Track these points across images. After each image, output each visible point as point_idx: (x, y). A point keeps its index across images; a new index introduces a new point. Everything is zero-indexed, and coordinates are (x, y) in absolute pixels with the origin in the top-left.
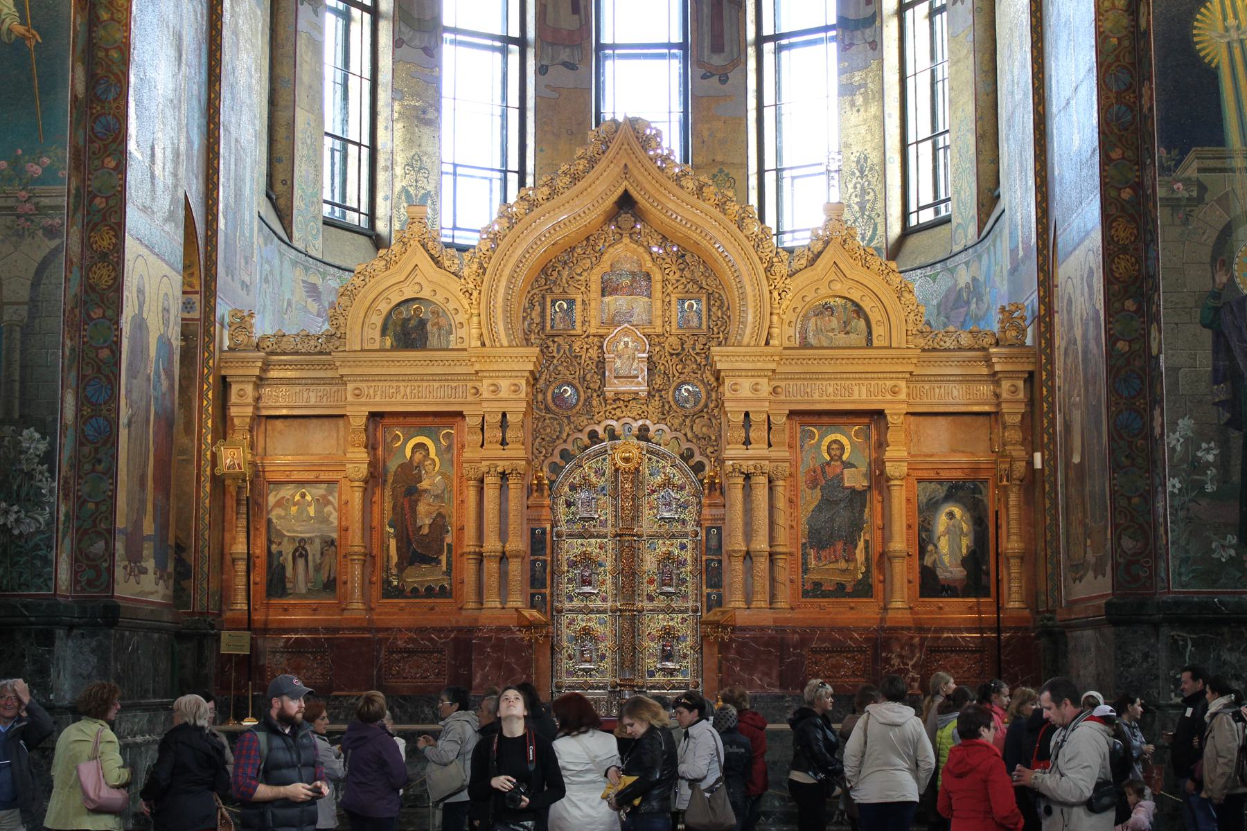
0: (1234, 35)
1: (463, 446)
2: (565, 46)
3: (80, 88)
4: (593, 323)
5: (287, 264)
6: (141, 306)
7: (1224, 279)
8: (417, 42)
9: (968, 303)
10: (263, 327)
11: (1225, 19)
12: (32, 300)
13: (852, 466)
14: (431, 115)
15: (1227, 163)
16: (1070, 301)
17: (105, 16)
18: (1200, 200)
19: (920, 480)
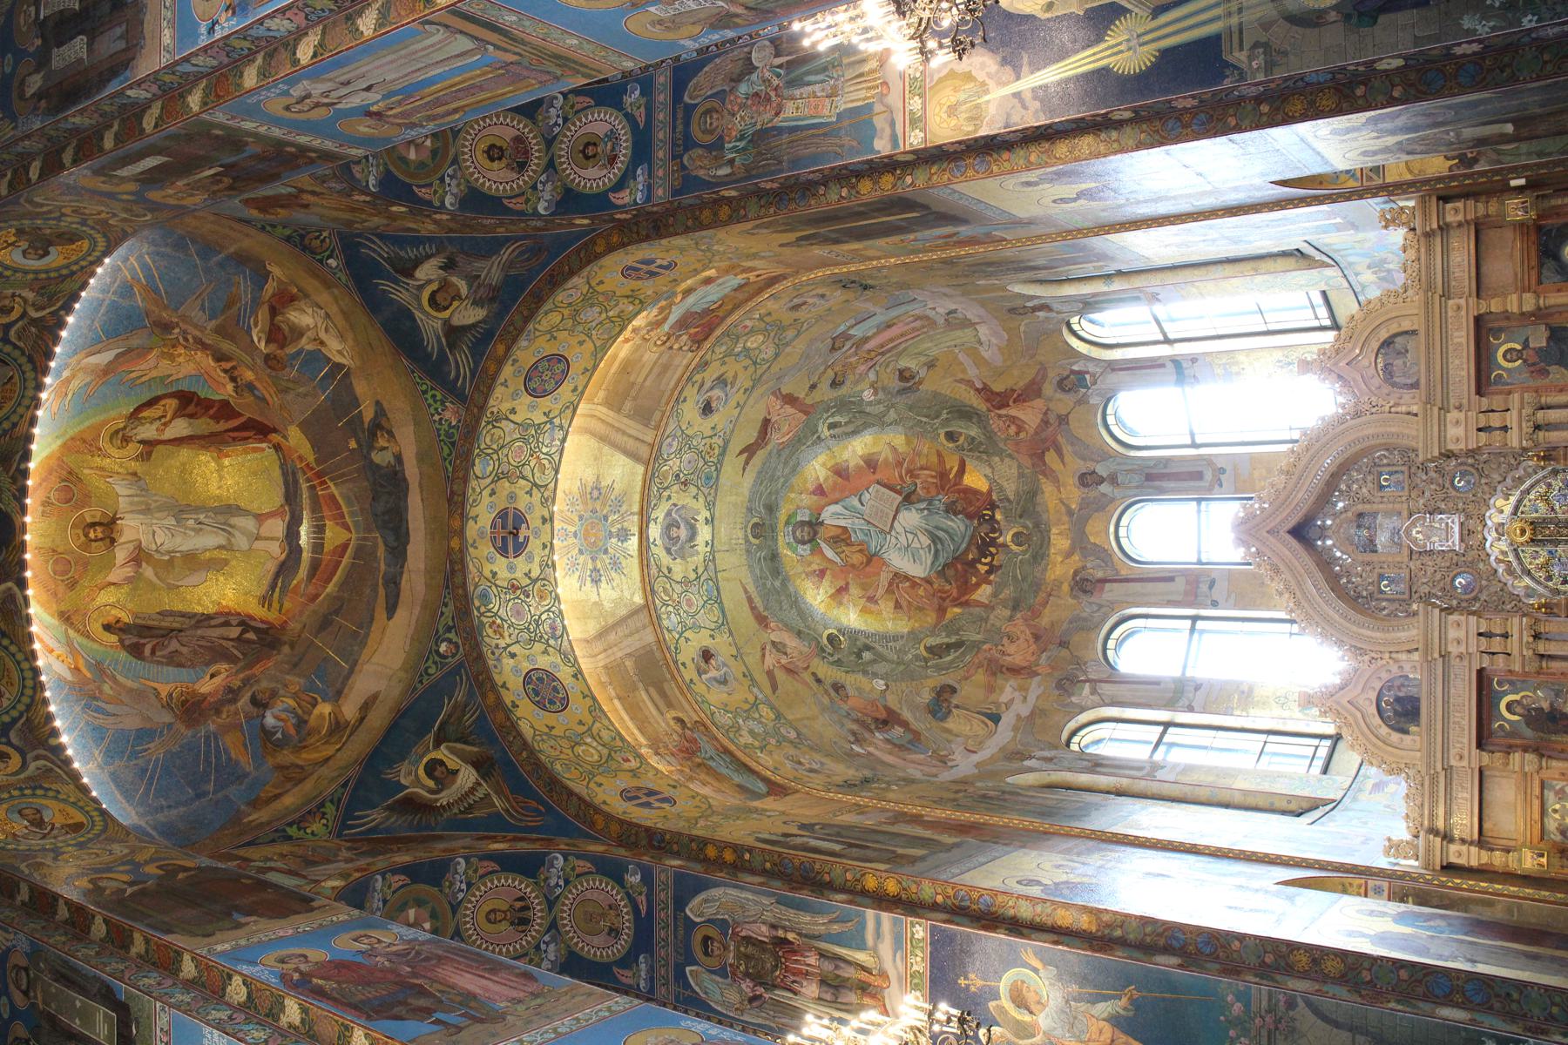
0: (1134, 43)
1: (1510, 671)
2: (1198, 587)
3: (1174, 960)
4: (1399, 559)
5: (1355, 806)
6: (1364, 935)
7: (1333, 13)
8: (1191, 695)
9: (1389, 271)
10: (1402, 832)
11: (1121, 52)
12: (1350, 1031)
13: (1527, 340)
14: (1246, 689)
15: (1235, 29)
16: (1365, 153)
17: (1118, 933)
18: (1266, 46)
19: (1540, 282)
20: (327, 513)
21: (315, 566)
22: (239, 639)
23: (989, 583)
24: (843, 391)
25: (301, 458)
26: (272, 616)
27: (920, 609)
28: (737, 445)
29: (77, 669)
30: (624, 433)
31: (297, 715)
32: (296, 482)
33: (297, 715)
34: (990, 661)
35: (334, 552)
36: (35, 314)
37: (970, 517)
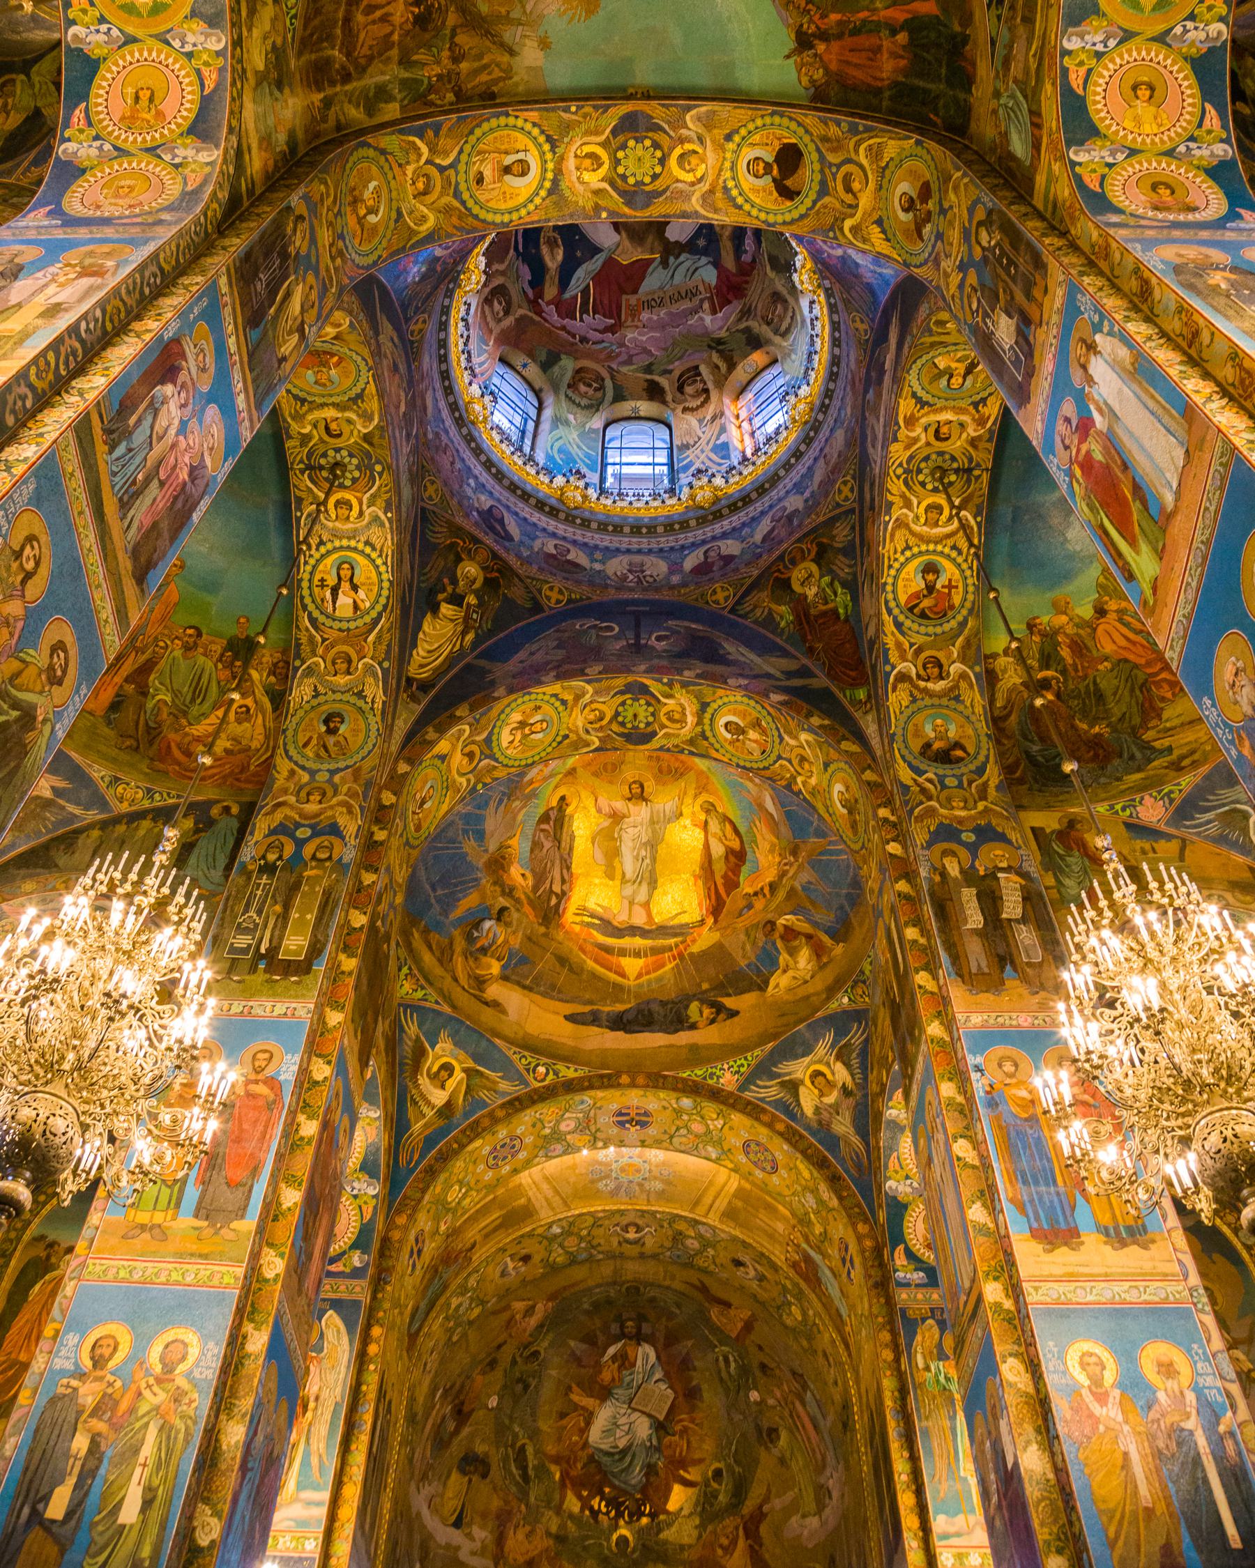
20: (651, 959)
21: (608, 950)
22: (551, 891)
23: (582, 1510)
24: (758, 1373)
25: (694, 941)
26: (570, 917)
27: (559, 1439)
28: (708, 1281)
29: (531, 782)
30: (716, 1198)
31: (491, 945)
32: (675, 935)
33: (491, 945)
34: (510, 1513)
35: (619, 966)
36: (799, 780)
37: (644, 1490)
